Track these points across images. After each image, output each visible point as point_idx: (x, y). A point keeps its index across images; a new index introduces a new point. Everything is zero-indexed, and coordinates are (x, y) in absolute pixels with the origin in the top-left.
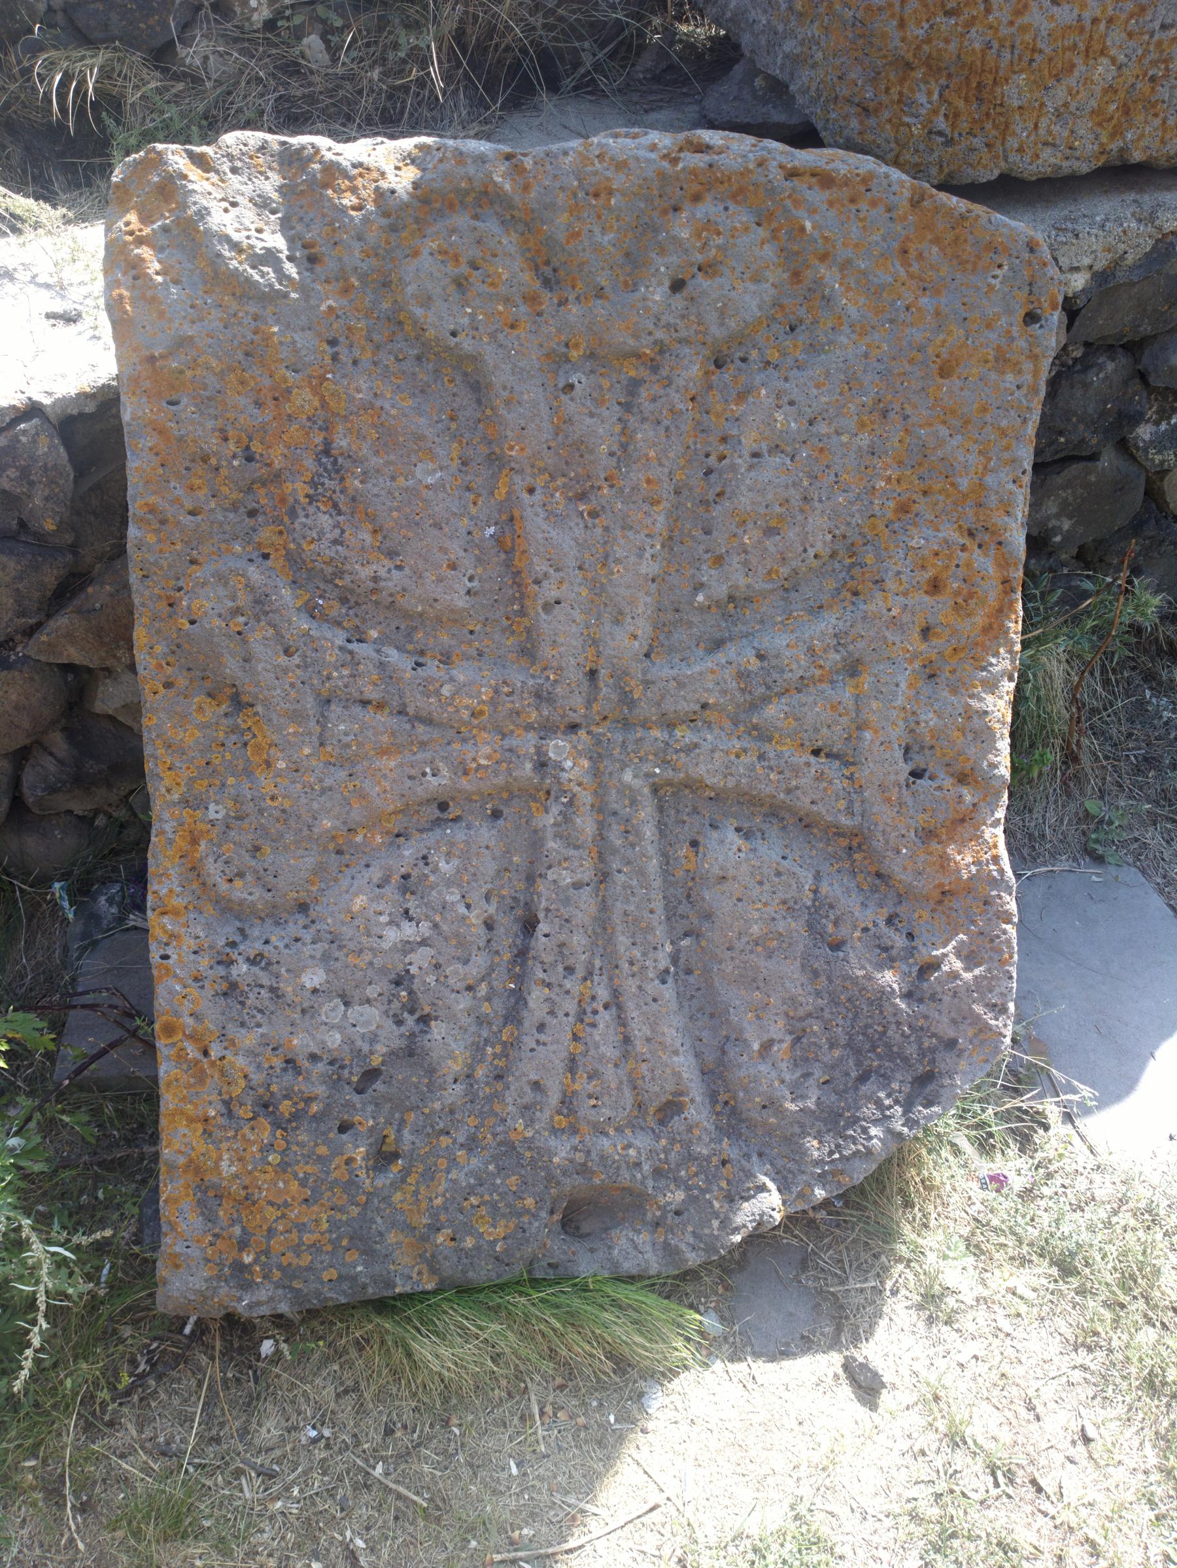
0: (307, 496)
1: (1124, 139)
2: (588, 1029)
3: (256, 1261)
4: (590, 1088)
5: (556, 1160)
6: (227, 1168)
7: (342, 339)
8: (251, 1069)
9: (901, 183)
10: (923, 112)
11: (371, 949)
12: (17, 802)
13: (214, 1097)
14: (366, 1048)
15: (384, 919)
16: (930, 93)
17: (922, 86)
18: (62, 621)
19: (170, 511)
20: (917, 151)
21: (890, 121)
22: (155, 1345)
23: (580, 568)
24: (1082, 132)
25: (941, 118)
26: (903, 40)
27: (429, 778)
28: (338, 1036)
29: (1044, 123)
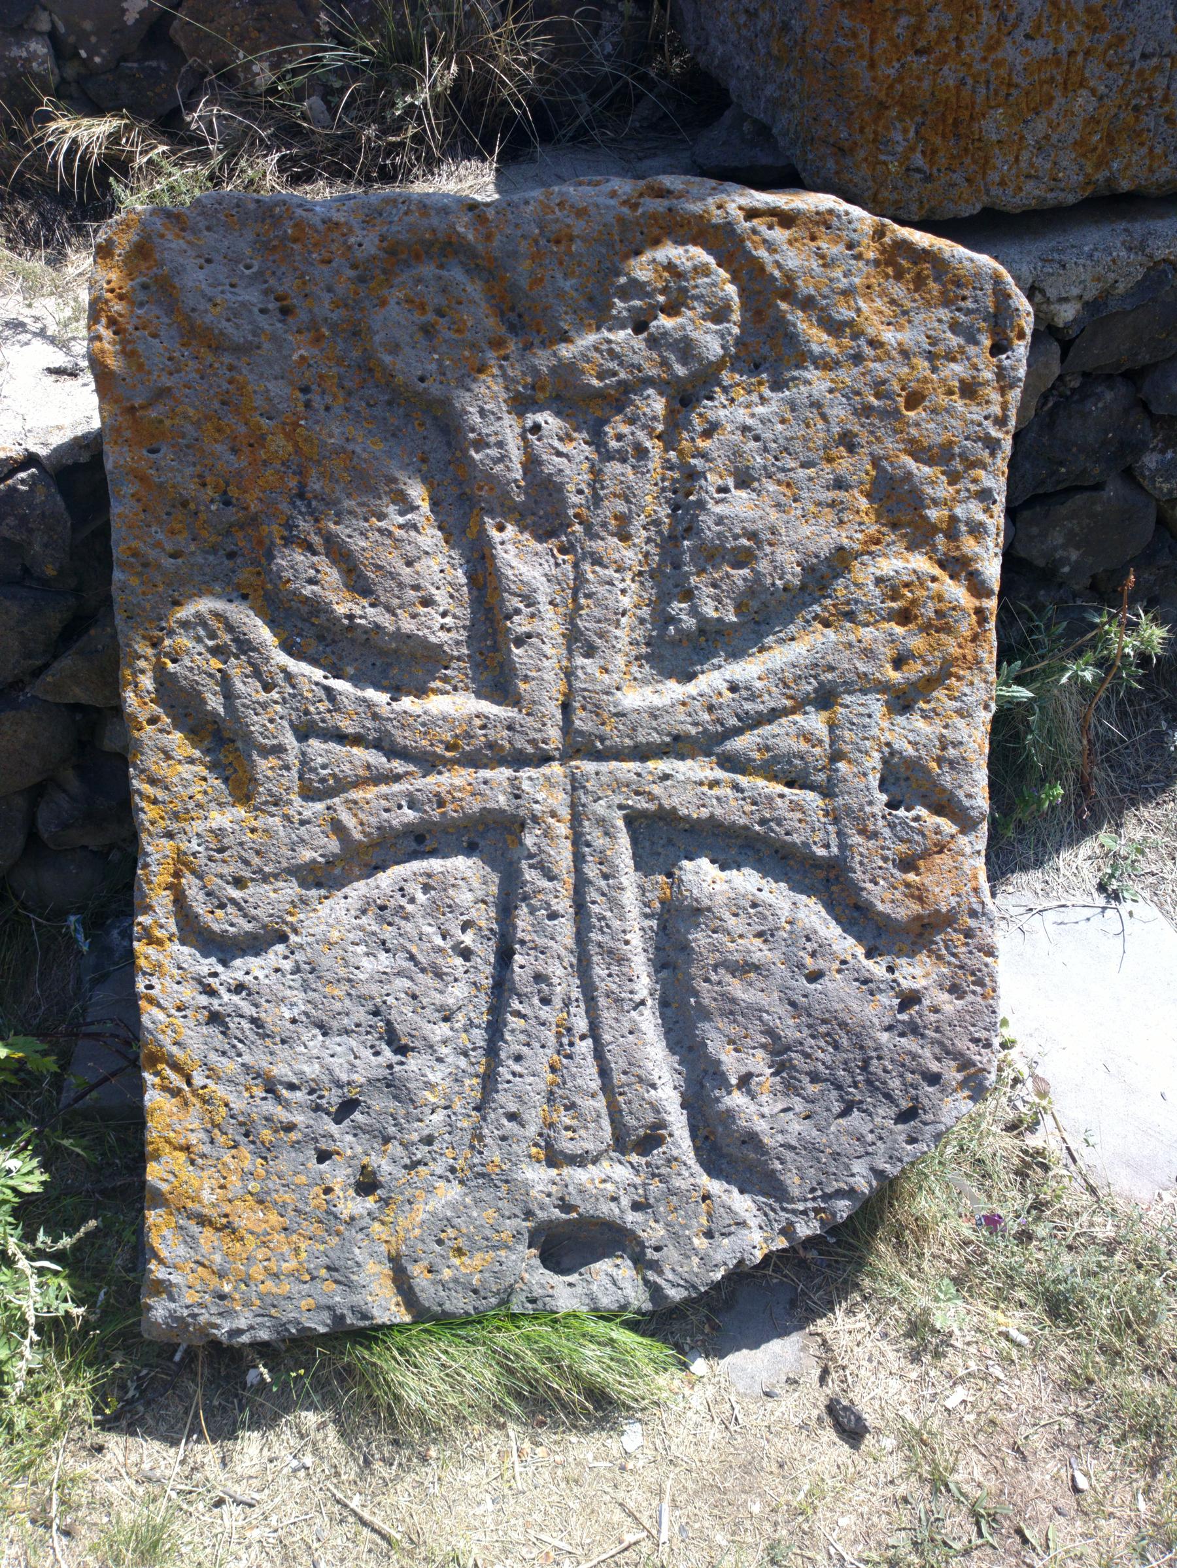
0: (282, 538)
1: (1110, 168)
2: (565, 1061)
3: (235, 1288)
4: (567, 1121)
5: (533, 1193)
6: (207, 1196)
7: (314, 387)
8: (231, 1098)
9: (861, 220)
11: (349, 980)
12: (33, 837)
13: (196, 1125)
14: (344, 1077)
15: (361, 949)
16: (905, 131)
17: (898, 125)
18: (66, 663)
19: (152, 554)
20: (895, 188)
21: (866, 159)
22: (144, 1372)
23: (551, 603)
24: (1065, 163)
25: (918, 155)
26: (874, 80)
27: (405, 809)
28: (317, 1066)
29: (1025, 156)
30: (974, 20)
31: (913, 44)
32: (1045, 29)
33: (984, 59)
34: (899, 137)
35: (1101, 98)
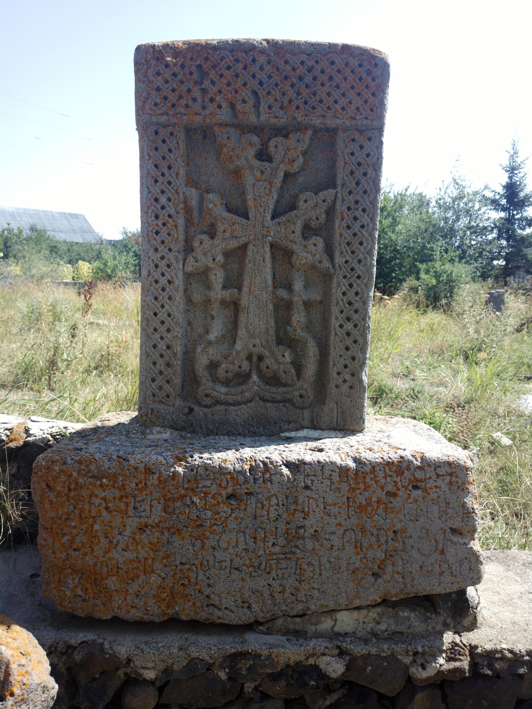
1: (175, 609)
10: (71, 586)
21: (55, 588)
24: (150, 604)
26: (55, 558)
29: (129, 598)
30: (97, 541)
32: (131, 548)
33: (104, 556)
34: (70, 582)
35: (164, 578)
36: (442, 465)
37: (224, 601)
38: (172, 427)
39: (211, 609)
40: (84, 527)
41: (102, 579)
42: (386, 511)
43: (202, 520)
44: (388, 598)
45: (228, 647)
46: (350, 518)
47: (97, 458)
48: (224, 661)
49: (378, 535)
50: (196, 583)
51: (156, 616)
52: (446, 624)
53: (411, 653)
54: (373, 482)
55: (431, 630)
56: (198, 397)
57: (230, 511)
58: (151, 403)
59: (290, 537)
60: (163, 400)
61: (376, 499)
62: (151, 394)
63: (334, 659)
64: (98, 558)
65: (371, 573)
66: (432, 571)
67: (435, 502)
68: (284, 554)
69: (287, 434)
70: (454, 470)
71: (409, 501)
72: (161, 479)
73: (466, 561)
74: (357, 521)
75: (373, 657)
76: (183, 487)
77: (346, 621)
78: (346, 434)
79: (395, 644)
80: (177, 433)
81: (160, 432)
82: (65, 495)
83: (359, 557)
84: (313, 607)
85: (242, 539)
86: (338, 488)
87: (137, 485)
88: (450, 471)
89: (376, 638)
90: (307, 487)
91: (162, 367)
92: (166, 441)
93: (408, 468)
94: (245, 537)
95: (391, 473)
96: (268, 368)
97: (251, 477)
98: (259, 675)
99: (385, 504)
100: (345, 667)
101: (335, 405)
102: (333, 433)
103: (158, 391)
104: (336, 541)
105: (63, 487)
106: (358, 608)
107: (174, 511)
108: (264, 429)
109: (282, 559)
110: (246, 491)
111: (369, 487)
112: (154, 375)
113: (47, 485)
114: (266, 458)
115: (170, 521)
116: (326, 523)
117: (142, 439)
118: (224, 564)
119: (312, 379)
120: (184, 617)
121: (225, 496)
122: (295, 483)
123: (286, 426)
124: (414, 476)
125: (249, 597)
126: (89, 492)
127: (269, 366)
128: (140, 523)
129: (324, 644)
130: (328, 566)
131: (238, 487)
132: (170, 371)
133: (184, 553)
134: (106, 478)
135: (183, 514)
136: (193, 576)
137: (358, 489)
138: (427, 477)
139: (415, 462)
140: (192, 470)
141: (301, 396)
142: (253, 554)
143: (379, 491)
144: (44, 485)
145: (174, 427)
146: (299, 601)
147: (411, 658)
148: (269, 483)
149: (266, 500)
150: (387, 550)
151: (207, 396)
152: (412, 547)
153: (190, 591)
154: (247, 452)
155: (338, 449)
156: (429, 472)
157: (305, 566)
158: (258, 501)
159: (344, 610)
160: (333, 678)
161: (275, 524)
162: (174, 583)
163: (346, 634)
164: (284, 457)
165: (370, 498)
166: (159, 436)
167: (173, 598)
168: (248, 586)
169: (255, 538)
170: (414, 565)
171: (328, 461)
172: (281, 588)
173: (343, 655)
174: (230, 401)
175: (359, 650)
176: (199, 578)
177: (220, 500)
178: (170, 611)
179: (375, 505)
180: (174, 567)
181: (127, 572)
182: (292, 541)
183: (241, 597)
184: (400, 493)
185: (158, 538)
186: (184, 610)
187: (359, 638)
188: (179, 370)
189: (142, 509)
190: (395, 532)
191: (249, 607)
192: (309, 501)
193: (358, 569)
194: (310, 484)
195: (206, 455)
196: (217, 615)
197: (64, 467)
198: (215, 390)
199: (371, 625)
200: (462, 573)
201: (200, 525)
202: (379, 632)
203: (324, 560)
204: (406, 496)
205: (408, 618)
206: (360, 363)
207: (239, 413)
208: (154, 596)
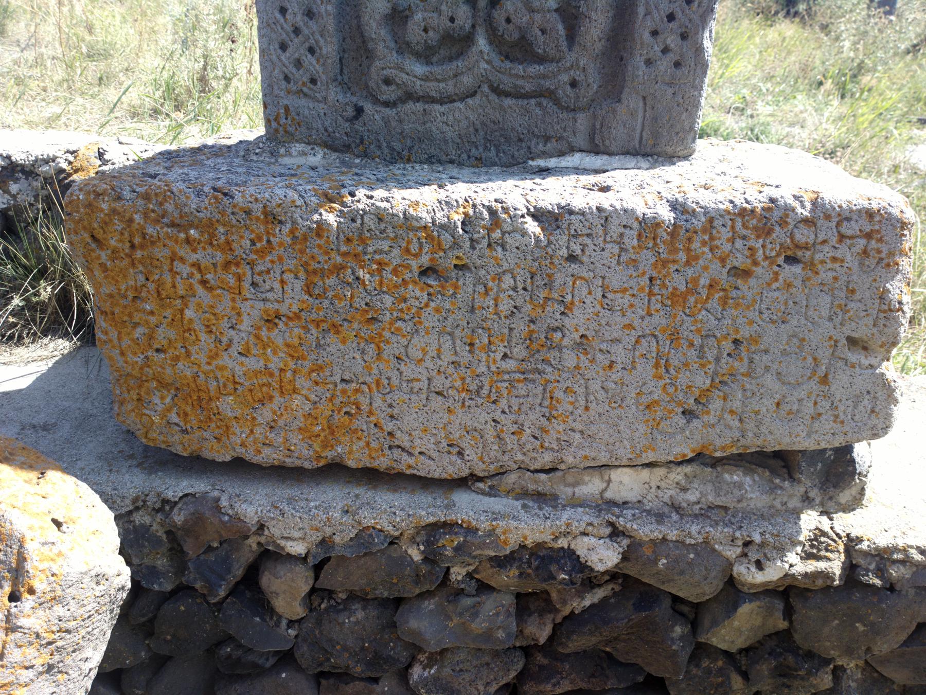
1: (336, 451)
10: (159, 409)
16: (162, 398)
21: (133, 410)
24: (294, 441)
25: (175, 416)
26: (126, 362)
29: (258, 431)
30: (194, 337)
31: (150, 346)
32: (254, 352)
33: (209, 364)
34: (157, 400)
36: (855, 217)
37: (417, 442)
38: (325, 145)
39: (397, 453)
40: (168, 313)
41: (210, 399)
42: (725, 303)
43: (376, 311)
44: (707, 453)
45: (423, 513)
46: (651, 315)
47: (175, 189)
48: (418, 533)
49: (702, 347)
50: (371, 413)
51: (306, 460)
52: (808, 498)
53: (740, 543)
54: (706, 249)
55: (779, 506)
56: (372, 84)
57: (426, 297)
58: (282, 94)
59: (535, 346)
60: (305, 89)
61: (708, 282)
62: (281, 77)
63: (601, 542)
64: (199, 366)
65: (681, 410)
66: (798, 411)
67: (826, 288)
68: (524, 373)
69: (542, 163)
70: (877, 227)
71: (775, 285)
72: (297, 234)
73: (867, 397)
74: (664, 322)
75: (671, 545)
76: (338, 250)
77: (626, 484)
78: (656, 161)
79: (711, 526)
80: (335, 155)
81: (304, 154)
82: (126, 255)
83: (661, 383)
84: (570, 460)
85: (448, 345)
86: (635, 261)
87: (253, 243)
88: (868, 229)
89: (678, 512)
90: (572, 258)
91: (299, 18)
92: (313, 169)
93: (783, 223)
94: (454, 343)
95: (744, 232)
96: (508, 20)
97: (466, 236)
98: (475, 557)
99: (724, 290)
100: (620, 556)
101: (641, 104)
102: (631, 161)
103: (294, 70)
104: (620, 354)
105: (120, 241)
106: (650, 465)
107: (325, 294)
108: (498, 152)
109: (519, 381)
110: (455, 262)
111: (697, 258)
112: (284, 36)
113: (92, 236)
114: (496, 201)
115: (319, 309)
116: (603, 322)
117: (269, 164)
118: (416, 385)
119: (599, 46)
120: (352, 464)
121: (416, 271)
122: (549, 250)
123: (541, 147)
124: (792, 237)
125: (460, 438)
126: (167, 252)
127: (512, 17)
128: (266, 311)
129: (586, 518)
130: (601, 395)
131: (442, 254)
132: (315, 28)
133: (347, 364)
134: (197, 228)
135: (340, 299)
136: (364, 402)
137: (674, 261)
138: (820, 239)
139: (799, 210)
140: (353, 220)
141: (574, 84)
142: (468, 371)
143: (716, 266)
144: (87, 237)
145: (330, 145)
146: (547, 449)
147: (739, 551)
148: (499, 249)
149: (493, 280)
150: (716, 373)
151: (388, 82)
152: (767, 369)
153: (360, 423)
154: (460, 190)
155: (641, 187)
156: (827, 231)
157: (559, 394)
158: (478, 281)
159: (624, 466)
160: (598, 572)
161: (508, 322)
162: (333, 411)
163: (625, 503)
164: (532, 200)
165: (695, 280)
166: (301, 160)
167: (333, 433)
168: (458, 422)
169: (471, 345)
170: (764, 401)
171: (618, 207)
172: (516, 426)
173: (618, 536)
174: (433, 94)
175: (647, 531)
176: (375, 405)
177: (407, 276)
178: (329, 454)
179: (704, 293)
180: (331, 386)
181: (251, 391)
182: (538, 351)
183: (446, 437)
184: (758, 270)
185: (300, 338)
186: (351, 452)
187: (649, 512)
188: (331, 24)
189: (268, 287)
190: (736, 342)
191: (460, 454)
192: (574, 283)
193: (656, 402)
194: (579, 252)
195: (379, 193)
196: (405, 463)
197: (118, 205)
198: (402, 70)
199: (672, 492)
200: (856, 418)
201: (373, 318)
202: (684, 505)
203: (595, 386)
204: (769, 276)
205: (740, 486)
206: (701, 11)
207: (451, 118)
208: (300, 429)
